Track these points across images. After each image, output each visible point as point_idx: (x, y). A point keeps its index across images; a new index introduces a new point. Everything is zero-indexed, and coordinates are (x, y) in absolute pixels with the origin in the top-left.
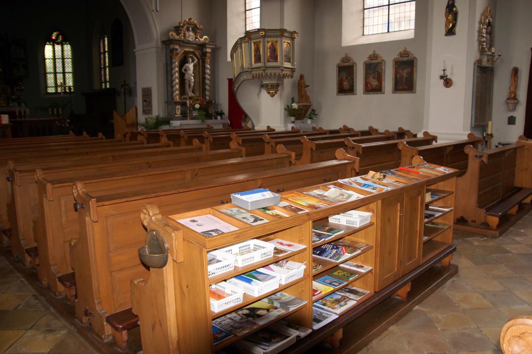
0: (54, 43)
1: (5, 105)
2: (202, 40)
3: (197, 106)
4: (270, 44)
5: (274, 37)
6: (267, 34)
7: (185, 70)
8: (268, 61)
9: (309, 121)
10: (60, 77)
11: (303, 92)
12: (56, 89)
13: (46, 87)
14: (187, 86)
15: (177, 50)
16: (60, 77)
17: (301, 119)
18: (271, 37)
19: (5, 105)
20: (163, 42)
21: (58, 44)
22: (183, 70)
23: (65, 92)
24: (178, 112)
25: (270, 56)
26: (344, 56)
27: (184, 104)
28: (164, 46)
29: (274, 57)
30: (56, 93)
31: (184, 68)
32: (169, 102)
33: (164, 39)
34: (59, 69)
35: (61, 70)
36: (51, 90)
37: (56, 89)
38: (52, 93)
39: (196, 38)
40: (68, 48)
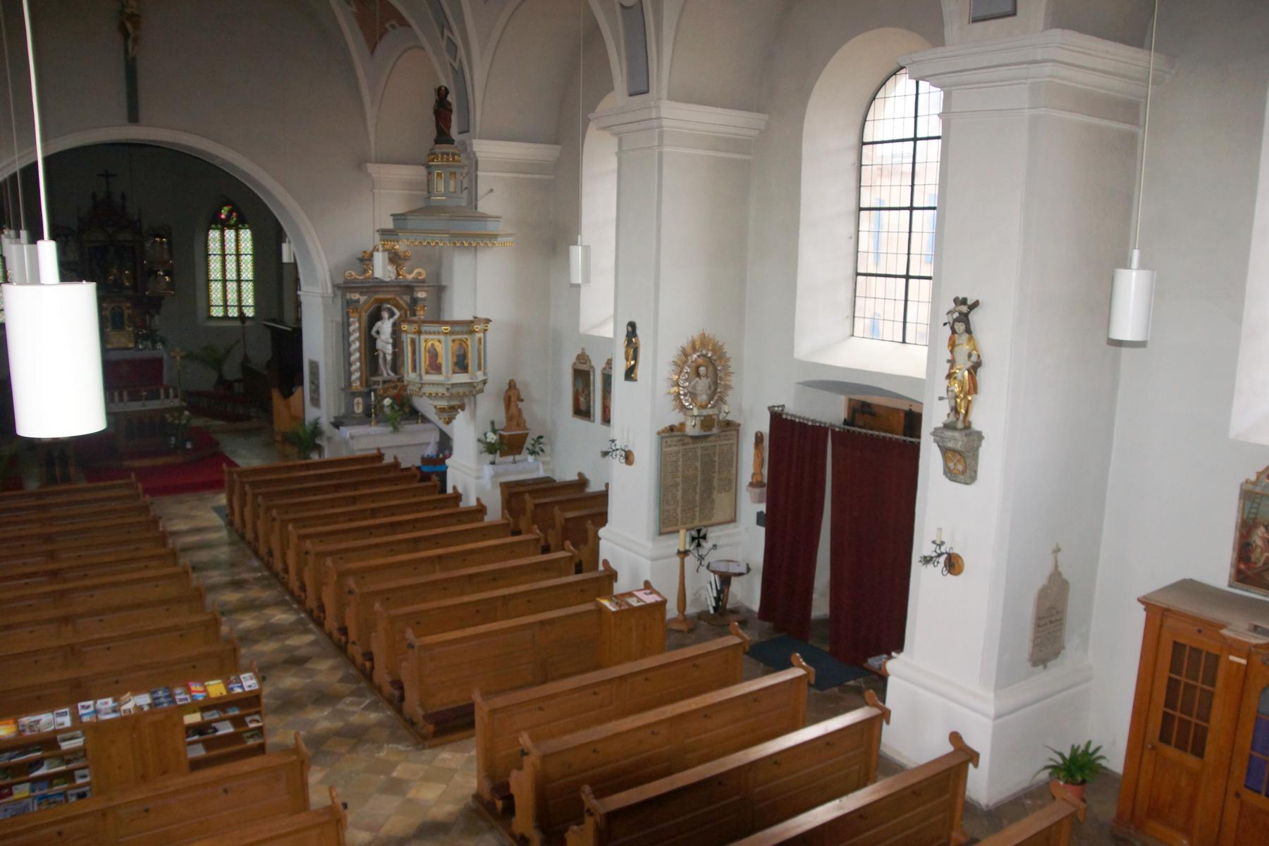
0: (224, 225)
1: (131, 345)
2: (410, 277)
3: (387, 402)
4: (429, 344)
5: (434, 333)
6: (424, 328)
7: (378, 332)
8: (427, 373)
9: (531, 459)
10: (232, 287)
11: (513, 410)
12: (226, 311)
13: (209, 306)
14: (381, 361)
15: (358, 301)
16: (232, 287)
17: (513, 454)
18: (430, 333)
19: (131, 345)
20: (336, 287)
21: (230, 227)
22: (373, 333)
23: (242, 317)
24: (359, 409)
25: (430, 365)
26: (579, 352)
27: (366, 395)
28: (339, 293)
29: (435, 367)
30: (226, 317)
31: (375, 329)
32: (348, 392)
33: (340, 281)
34: (231, 275)
35: (234, 276)
36: (217, 312)
37: (226, 311)
38: (218, 318)
39: (398, 274)
40: (246, 235)
